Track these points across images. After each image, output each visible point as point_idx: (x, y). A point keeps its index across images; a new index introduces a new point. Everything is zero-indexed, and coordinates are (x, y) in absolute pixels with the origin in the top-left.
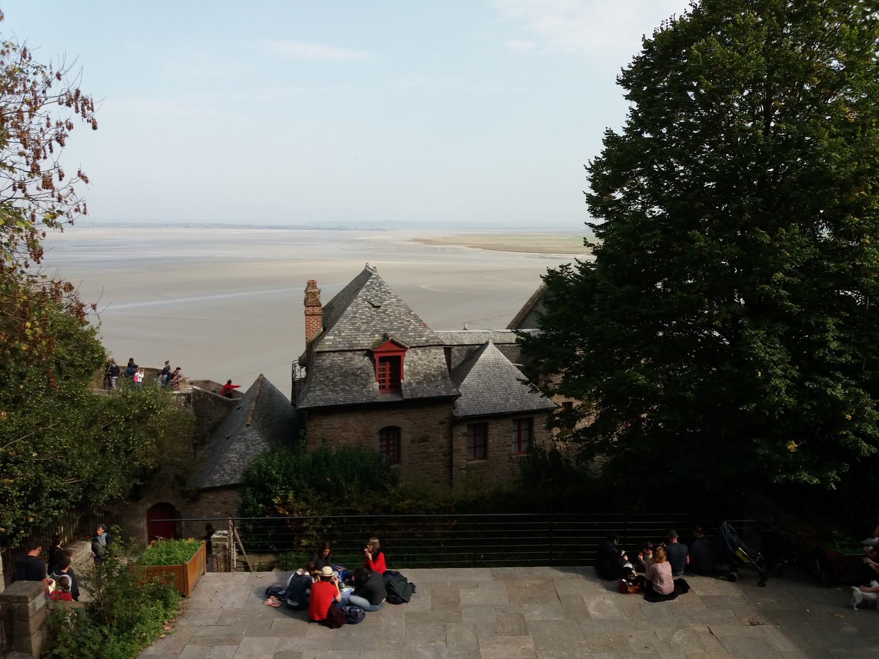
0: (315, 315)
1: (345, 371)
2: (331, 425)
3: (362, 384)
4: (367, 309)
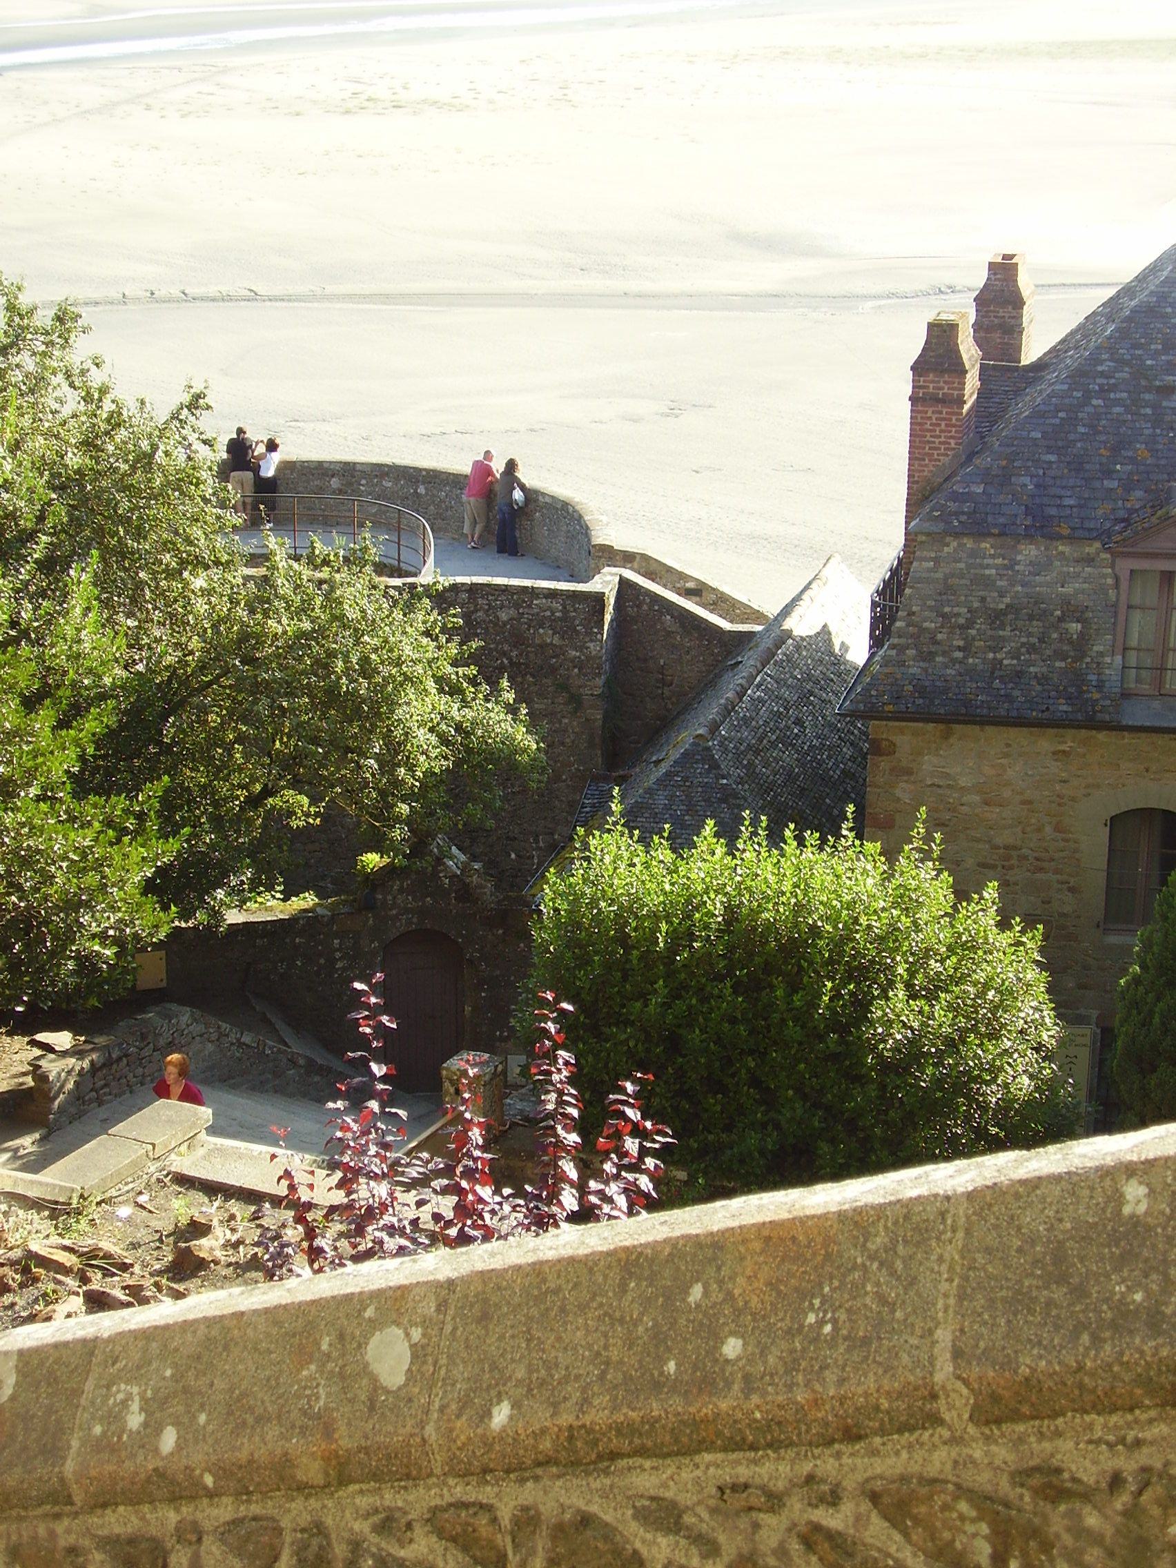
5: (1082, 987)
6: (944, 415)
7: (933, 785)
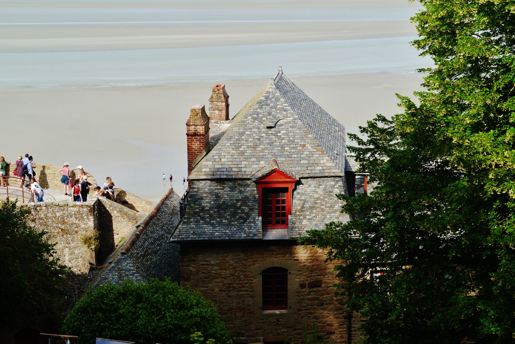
0: (197, 135)
1: (224, 202)
2: (207, 261)
3: (241, 218)
4: (256, 130)
5: (257, 329)
6: (198, 139)
7: (202, 264)
